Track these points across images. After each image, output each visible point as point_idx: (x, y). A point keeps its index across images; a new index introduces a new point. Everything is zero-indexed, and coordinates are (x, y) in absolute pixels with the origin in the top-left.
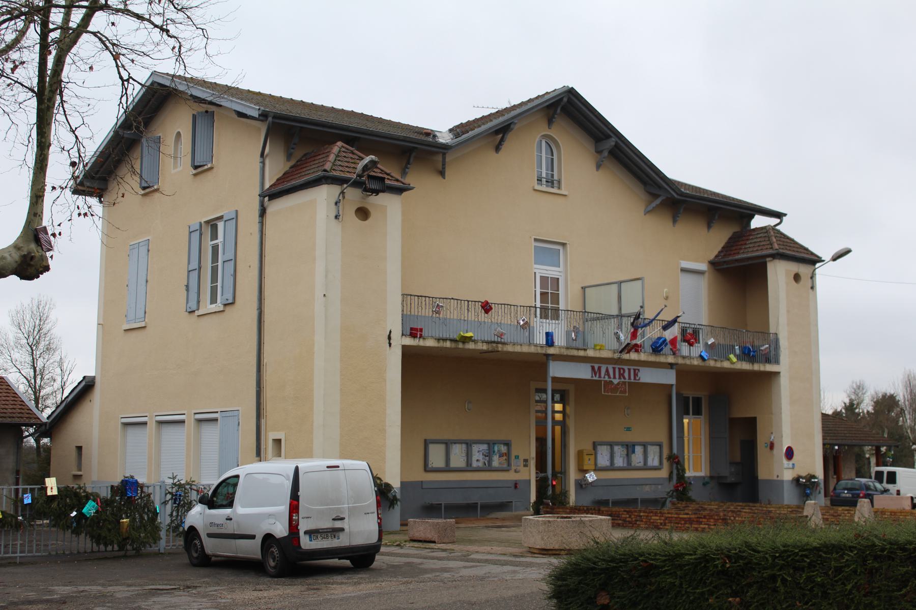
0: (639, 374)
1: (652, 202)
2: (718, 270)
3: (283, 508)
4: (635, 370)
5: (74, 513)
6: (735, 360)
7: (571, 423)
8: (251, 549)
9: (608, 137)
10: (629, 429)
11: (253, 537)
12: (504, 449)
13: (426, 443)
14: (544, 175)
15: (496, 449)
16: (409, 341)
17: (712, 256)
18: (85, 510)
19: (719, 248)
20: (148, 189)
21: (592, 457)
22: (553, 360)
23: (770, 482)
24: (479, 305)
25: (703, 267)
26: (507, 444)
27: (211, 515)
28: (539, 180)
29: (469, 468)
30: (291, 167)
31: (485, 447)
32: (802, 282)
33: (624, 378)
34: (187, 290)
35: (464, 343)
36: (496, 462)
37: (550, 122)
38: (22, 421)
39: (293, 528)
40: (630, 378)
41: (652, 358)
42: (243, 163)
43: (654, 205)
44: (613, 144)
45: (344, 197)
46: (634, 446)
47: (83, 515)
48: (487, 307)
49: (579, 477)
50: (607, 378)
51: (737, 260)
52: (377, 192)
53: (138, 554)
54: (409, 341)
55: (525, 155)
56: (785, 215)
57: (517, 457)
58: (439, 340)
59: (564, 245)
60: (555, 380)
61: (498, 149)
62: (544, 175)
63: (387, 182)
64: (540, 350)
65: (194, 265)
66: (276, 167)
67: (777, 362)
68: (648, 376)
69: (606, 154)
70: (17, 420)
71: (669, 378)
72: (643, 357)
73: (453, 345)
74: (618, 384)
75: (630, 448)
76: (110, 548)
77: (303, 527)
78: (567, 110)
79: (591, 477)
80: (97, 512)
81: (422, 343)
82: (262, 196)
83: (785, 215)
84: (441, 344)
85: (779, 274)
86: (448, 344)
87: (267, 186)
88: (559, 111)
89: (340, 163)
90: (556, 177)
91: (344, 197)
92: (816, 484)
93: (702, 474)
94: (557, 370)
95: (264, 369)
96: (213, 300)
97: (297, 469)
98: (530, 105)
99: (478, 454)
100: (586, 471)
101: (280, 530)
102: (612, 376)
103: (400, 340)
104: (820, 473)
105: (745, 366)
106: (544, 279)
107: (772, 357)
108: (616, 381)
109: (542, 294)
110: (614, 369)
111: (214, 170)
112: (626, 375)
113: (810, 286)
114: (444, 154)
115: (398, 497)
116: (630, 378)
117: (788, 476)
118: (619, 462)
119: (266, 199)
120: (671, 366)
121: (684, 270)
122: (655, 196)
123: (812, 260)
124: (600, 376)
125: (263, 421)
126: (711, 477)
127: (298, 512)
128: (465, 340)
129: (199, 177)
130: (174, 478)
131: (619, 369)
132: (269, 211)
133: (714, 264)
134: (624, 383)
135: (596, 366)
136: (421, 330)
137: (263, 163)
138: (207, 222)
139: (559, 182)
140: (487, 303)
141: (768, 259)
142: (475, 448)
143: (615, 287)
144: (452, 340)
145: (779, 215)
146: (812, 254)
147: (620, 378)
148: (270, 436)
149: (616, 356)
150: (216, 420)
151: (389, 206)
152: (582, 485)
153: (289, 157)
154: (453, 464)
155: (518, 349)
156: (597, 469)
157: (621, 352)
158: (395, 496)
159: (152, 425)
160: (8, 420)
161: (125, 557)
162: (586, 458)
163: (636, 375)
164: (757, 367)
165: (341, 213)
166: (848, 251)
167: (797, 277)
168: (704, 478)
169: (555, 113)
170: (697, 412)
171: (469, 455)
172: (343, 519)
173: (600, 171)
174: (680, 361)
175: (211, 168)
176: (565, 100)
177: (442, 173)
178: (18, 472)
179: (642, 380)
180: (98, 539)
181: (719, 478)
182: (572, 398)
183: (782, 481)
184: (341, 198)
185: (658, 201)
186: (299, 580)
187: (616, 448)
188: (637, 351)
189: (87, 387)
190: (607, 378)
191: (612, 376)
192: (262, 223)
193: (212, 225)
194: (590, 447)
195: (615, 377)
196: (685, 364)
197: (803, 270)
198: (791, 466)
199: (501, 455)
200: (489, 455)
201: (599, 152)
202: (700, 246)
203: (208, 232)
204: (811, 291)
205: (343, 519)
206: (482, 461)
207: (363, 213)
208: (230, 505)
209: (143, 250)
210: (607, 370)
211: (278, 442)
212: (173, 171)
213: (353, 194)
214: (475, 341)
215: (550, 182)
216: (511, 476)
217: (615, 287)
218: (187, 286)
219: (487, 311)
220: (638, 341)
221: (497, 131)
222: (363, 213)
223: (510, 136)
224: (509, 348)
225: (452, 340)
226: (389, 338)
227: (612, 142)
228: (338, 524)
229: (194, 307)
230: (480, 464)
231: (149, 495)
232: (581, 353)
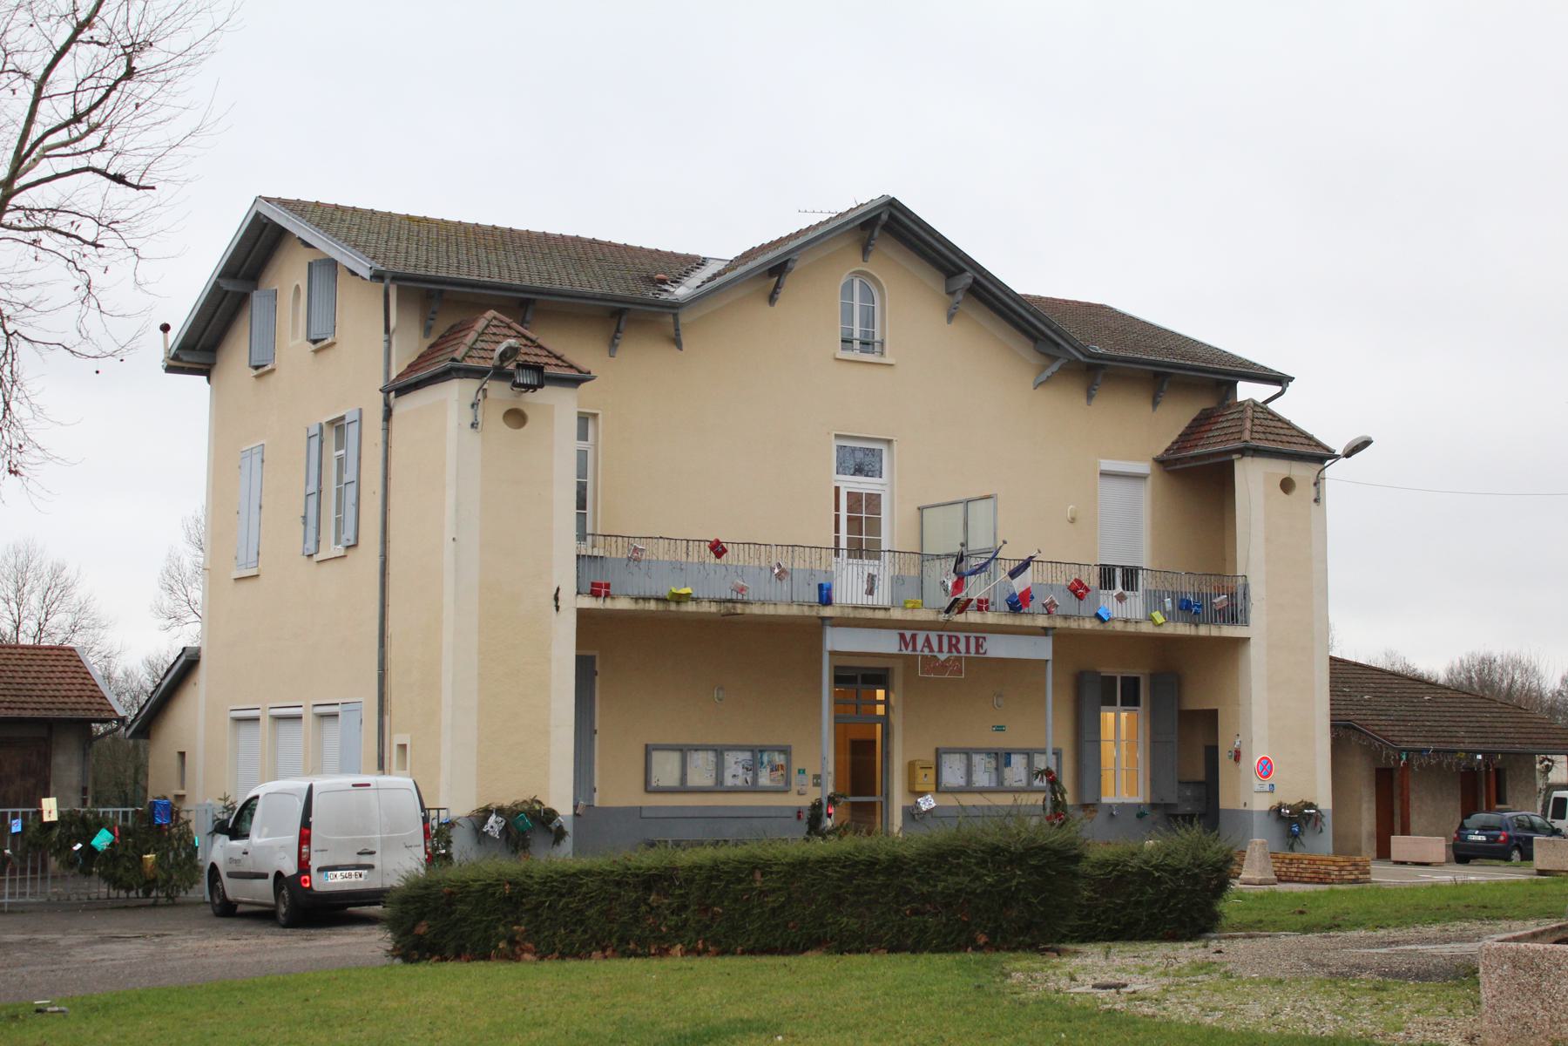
1: (1045, 367)
2: (1173, 473)
3: (293, 839)
4: (977, 639)
5: (79, 846)
6: (1160, 618)
7: (897, 720)
8: (263, 891)
9: (964, 271)
10: (1000, 729)
11: (265, 876)
12: (779, 759)
13: (648, 750)
14: (857, 335)
15: (765, 758)
16: (588, 603)
17: (1159, 451)
18: (95, 842)
19: (1175, 437)
20: (261, 370)
21: (932, 773)
22: (833, 626)
23: (1234, 813)
24: (705, 547)
25: (1144, 467)
26: (785, 751)
27: (234, 849)
28: (847, 342)
29: (719, 788)
30: (432, 346)
31: (747, 755)
32: (1296, 493)
34: (305, 523)
35: (678, 603)
36: (765, 779)
37: (866, 252)
38: (96, 715)
39: (304, 866)
40: (968, 650)
42: (369, 340)
43: (1048, 373)
44: (970, 281)
45: (485, 397)
46: (1009, 754)
47: (93, 850)
48: (718, 549)
49: (910, 803)
51: (1194, 458)
52: (534, 388)
53: (172, 902)
54: (588, 603)
56: (1292, 379)
57: (802, 771)
58: (637, 599)
59: (889, 442)
60: (833, 653)
61: (772, 299)
62: (857, 335)
63: (548, 370)
64: (806, 611)
65: (313, 488)
66: (409, 346)
67: (1246, 623)
68: (998, 647)
69: (960, 296)
70: (89, 715)
71: (1042, 649)
72: (990, 618)
73: (661, 607)
74: (948, 659)
75: (1002, 758)
76: (132, 894)
77: (315, 864)
78: (888, 228)
79: (927, 803)
80: (112, 844)
81: (609, 604)
82: (386, 391)
83: (1292, 379)
84: (641, 606)
85: (1253, 481)
86: (652, 606)
87: (394, 376)
88: (876, 234)
89: (483, 345)
90: (877, 338)
91: (485, 397)
92: (1317, 818)
93: (1139, 800)
94: (838, 641)
95: (388, 642)
96: (337, 542)
97: (311, 788)
98: (811, 235)
99: (735, 767)
100: (922, 794)
101: (290, 868)
102: (936, 648)
103: (573, 601)
104: (1324, 802)
105: (1183, 629)
106: (854, 498)
107: (1234, 613)
108: (943, 657)
109: (849, 519)
110: (940, 637)
111: (276, 374)
112: (962, 646)
113: (1313, 495)
114: (675, 315)
115: (568, 828)
116: (968, 650)
117: (1261, 803)
118: (982, 778)
119: (392, 394)
120: (1045, 631)
121: (1105, 474)
122: (1053, 359)
123: (1320, 456)
125: (387, 718)
126: (1153, 806)
127: (309, 843)
128: (679, 599)
129: (321, 354)
130: (225, 799)
131: (950, 638)
132: (395, 413)
133: (1164, 463)
134: (958, 659)
135: (908, 634)
136: (608, 586)
137: (389, 342)
138: (331, 423)
139: (882, 343)
140: (718, 542)
141: (1235, 457)
142: (730, 758)
143: (960, 507)
144: (658, 599)
145: (1281, 380)
146: (1319, 444)
147: (950, 651)
148: (395, 739)
149: (942, 617)
150: (336, 715)
151: (557, 407)
152: (912, 814)
153: (427, 331)
154: (729, 781)
155: (770, 610)
156: (939, 789)
157: (947, 611)
158: (560, 828)
159: (265, 722)
160: (67, 714)
161: (154, 905)
162: (920, 773)
163: (978, 646)
164: (1203, 631)
165: (480, 419)
166: (1366, 443)
167: (1287, 485)
168: (1139, 805)
169: (871, 237)
170: (1131, 700)
172: (372, 853)
174: (1059, 623)
175: (333, 344)
176: (885, 217)
177: (677, 342)
178: (85, 791)
179: (989, 655)
180: (115, 883)
181: (1166, 805)
182: (898, 681)
183: (1251, 812)
184: (480, 396)
185: (1055, 367)
186: (300, 931)
187: (976, 758)
188: (980, 609)
189: (188, 665)
191: (936, 648)
192: (387, 430)
193: (338, 425)
194: (932, 759)
195: (941, 650)
196: (1069, 629)
197: (1301, 472)
198: (1267, 788)
199: (774, 769)
200: (753, 768)
201: (951, 293)
202: (1140, 433)
203: (330, 438)
205: (372, 853)
207: (516, 417)
208: (247, 836)
209: (257, 459)
210: (928, 640)
211: (403, 747)
212: (291, 344)
213: (499, 391)
214: (697, 600)
215: (866, 344)
217: (960, 507)
218: (305, 517)
219: (719, 555)
220: (962, 596)
221: (771, 270)
222: (516, 417)
223: (788, 280)
224: (755, 610)
225: (658, 599)
226: (556, 598)
227: (967, 279)
228: (366, 860)
229: (312, 550)
230: (739, 782)
231: (187, 823)
232: (880, 615)
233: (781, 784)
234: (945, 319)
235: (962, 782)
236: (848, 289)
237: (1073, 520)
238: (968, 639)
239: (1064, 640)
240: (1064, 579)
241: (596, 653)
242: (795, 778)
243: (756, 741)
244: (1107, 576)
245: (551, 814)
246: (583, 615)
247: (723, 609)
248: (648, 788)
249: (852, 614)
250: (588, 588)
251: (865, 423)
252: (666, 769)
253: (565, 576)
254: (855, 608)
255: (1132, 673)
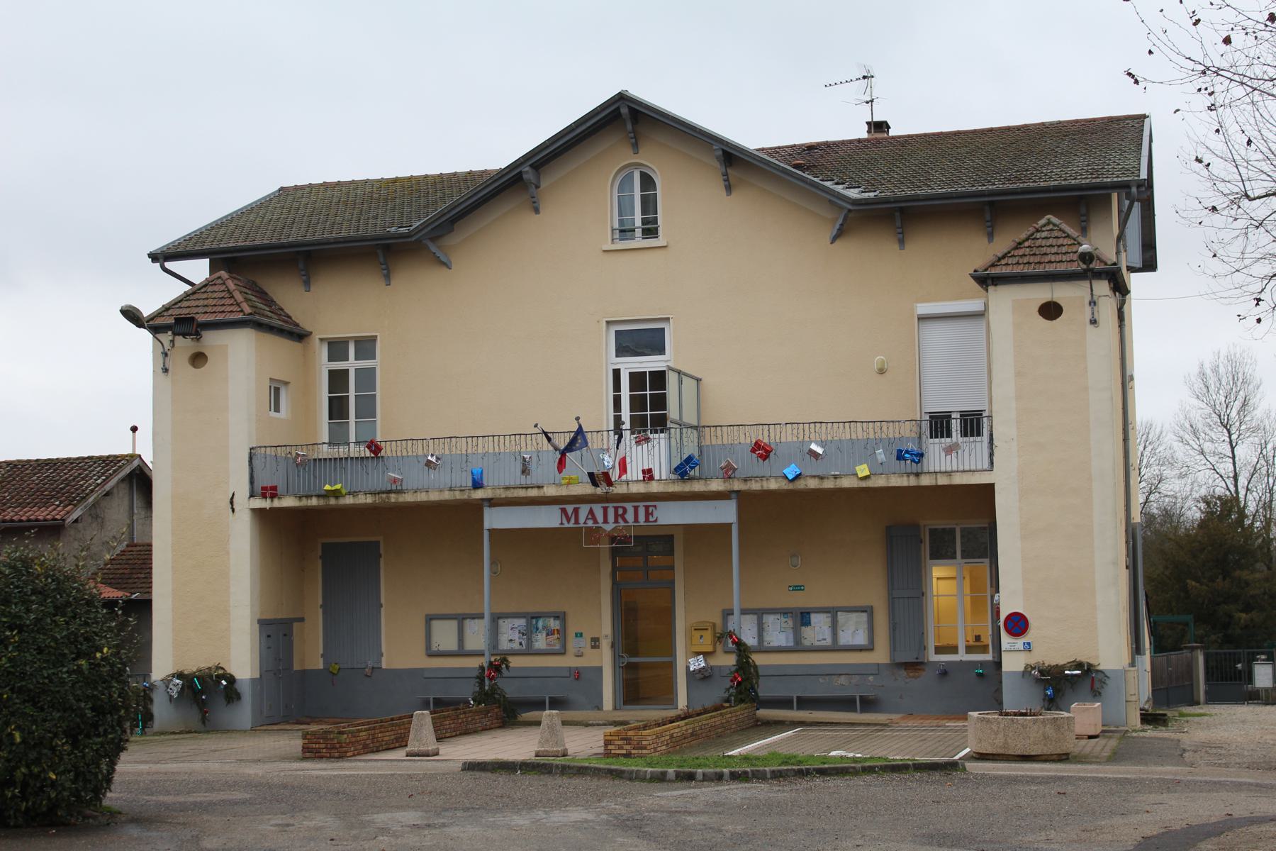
0: (656, 514)
4: (647, 508)
10: (798, 588)
12: (554, 624)
13: (430, 619)
14: (638, 223)
31: (522, 622)
33: (625, 521)
35: (337, 497)
36: (541, 642)
37: (635, 147)
40: (636, 520)
41: (677, 488)
50: (590, 523)
55: (588, 205)
60: (491, 531)
71: (726, 513)
75: (803, 617)
81: (277, 503)
84: (305, 503)
86: (314, 502)
94: (495, 519)
99: (510, 634)
102: (600, 518)
103: (246, 505)
108: (609, 527)
110: (605, 509)
112: (630, 516)
113: (1088, 317)
116: (636, 520)
121: (922, 318)
124: (577, 522)
128: (336, 494)
131: (616, 509)
142: (505, 625)
147: (616, 521)
163: (648, 514)
171: (494, 632)
173: (734, 194)
174: (737, 486)
179: (660, 522)
190: (590, 523)
191: (600, 518)
195: (606, 521)
199: (550, 633)
200: (528, 633)
204: (1090, 328)
206: (518, 641)
210: (591, 512)
216: (568, 661)
224: (408, 498)
226: (232, 502)
230: (516, 646)
232: (533, 493)
233: (558, 647)
234: (724, 193)
235: (829, 642)
236: (626, 184)
237: (882, 371)
238: (636, 508)
239: (746, 501)
240: (748, 438)
241: (380, 539)
242: (572, 643)
243: (460, 610)
244: (940, 425)
245: (231, 680)
246: (259, 513)
247: (377, 499)
248: (432, 654)
249: (503, 494)
250: (260, 491)
251: (638, 308)
252: (445, 636)
253: (241, 486)
254: (507, 488)
255: (940, 524)
